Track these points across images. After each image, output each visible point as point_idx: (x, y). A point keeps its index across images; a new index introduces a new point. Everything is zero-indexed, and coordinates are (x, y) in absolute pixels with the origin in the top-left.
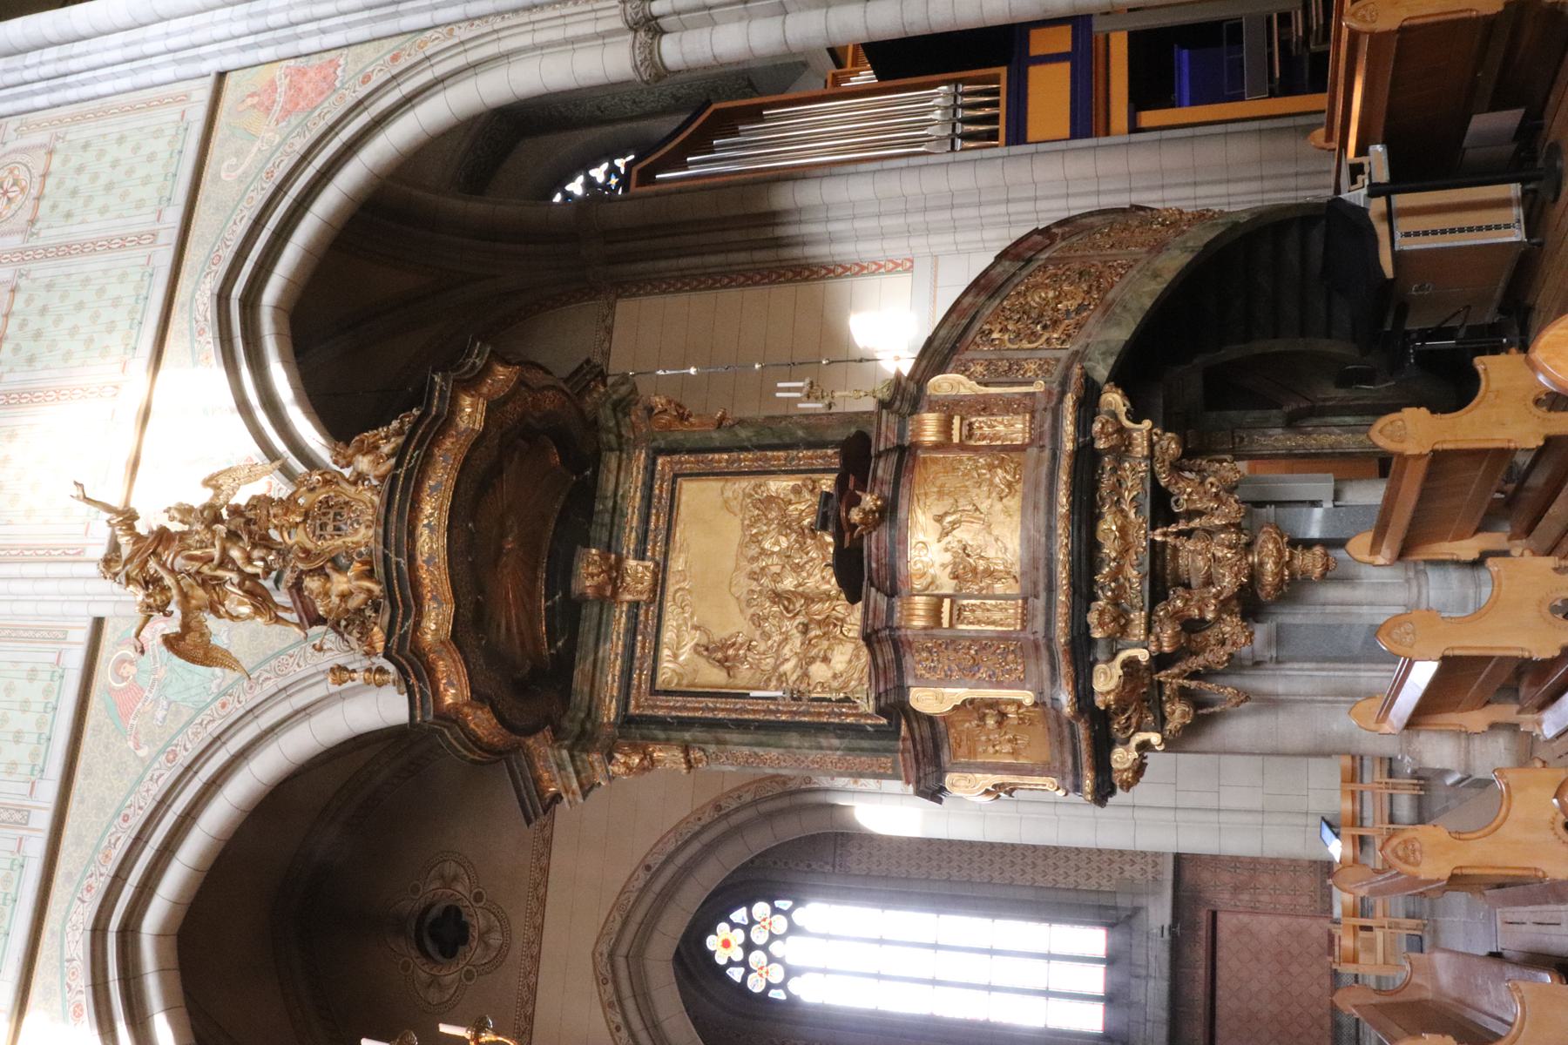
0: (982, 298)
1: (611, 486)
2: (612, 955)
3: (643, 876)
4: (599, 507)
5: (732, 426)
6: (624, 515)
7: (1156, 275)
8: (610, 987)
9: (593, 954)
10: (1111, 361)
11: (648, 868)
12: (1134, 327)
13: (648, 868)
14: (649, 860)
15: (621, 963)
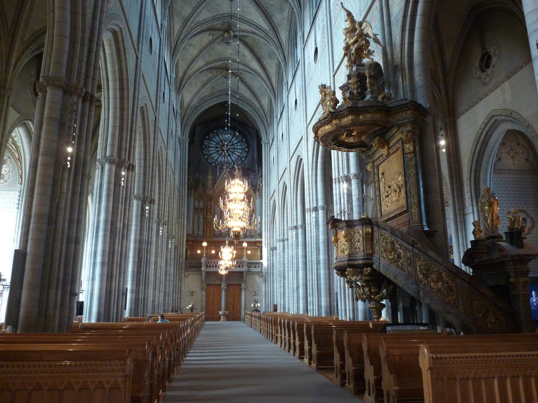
0: (390, 231)
1: (394, 132)
2: (493, 116)
3: (508, 113)
4: (390, 132)
5: (407, 157)
6: (394, 138)
7: (395, 277)
8: (487, 120)
9: (491, 111)
10: (376, 268)
11: (511, 114)
12: (383, 273)
13: (511, 114)
14: (513, 112)
15: (493, 120)
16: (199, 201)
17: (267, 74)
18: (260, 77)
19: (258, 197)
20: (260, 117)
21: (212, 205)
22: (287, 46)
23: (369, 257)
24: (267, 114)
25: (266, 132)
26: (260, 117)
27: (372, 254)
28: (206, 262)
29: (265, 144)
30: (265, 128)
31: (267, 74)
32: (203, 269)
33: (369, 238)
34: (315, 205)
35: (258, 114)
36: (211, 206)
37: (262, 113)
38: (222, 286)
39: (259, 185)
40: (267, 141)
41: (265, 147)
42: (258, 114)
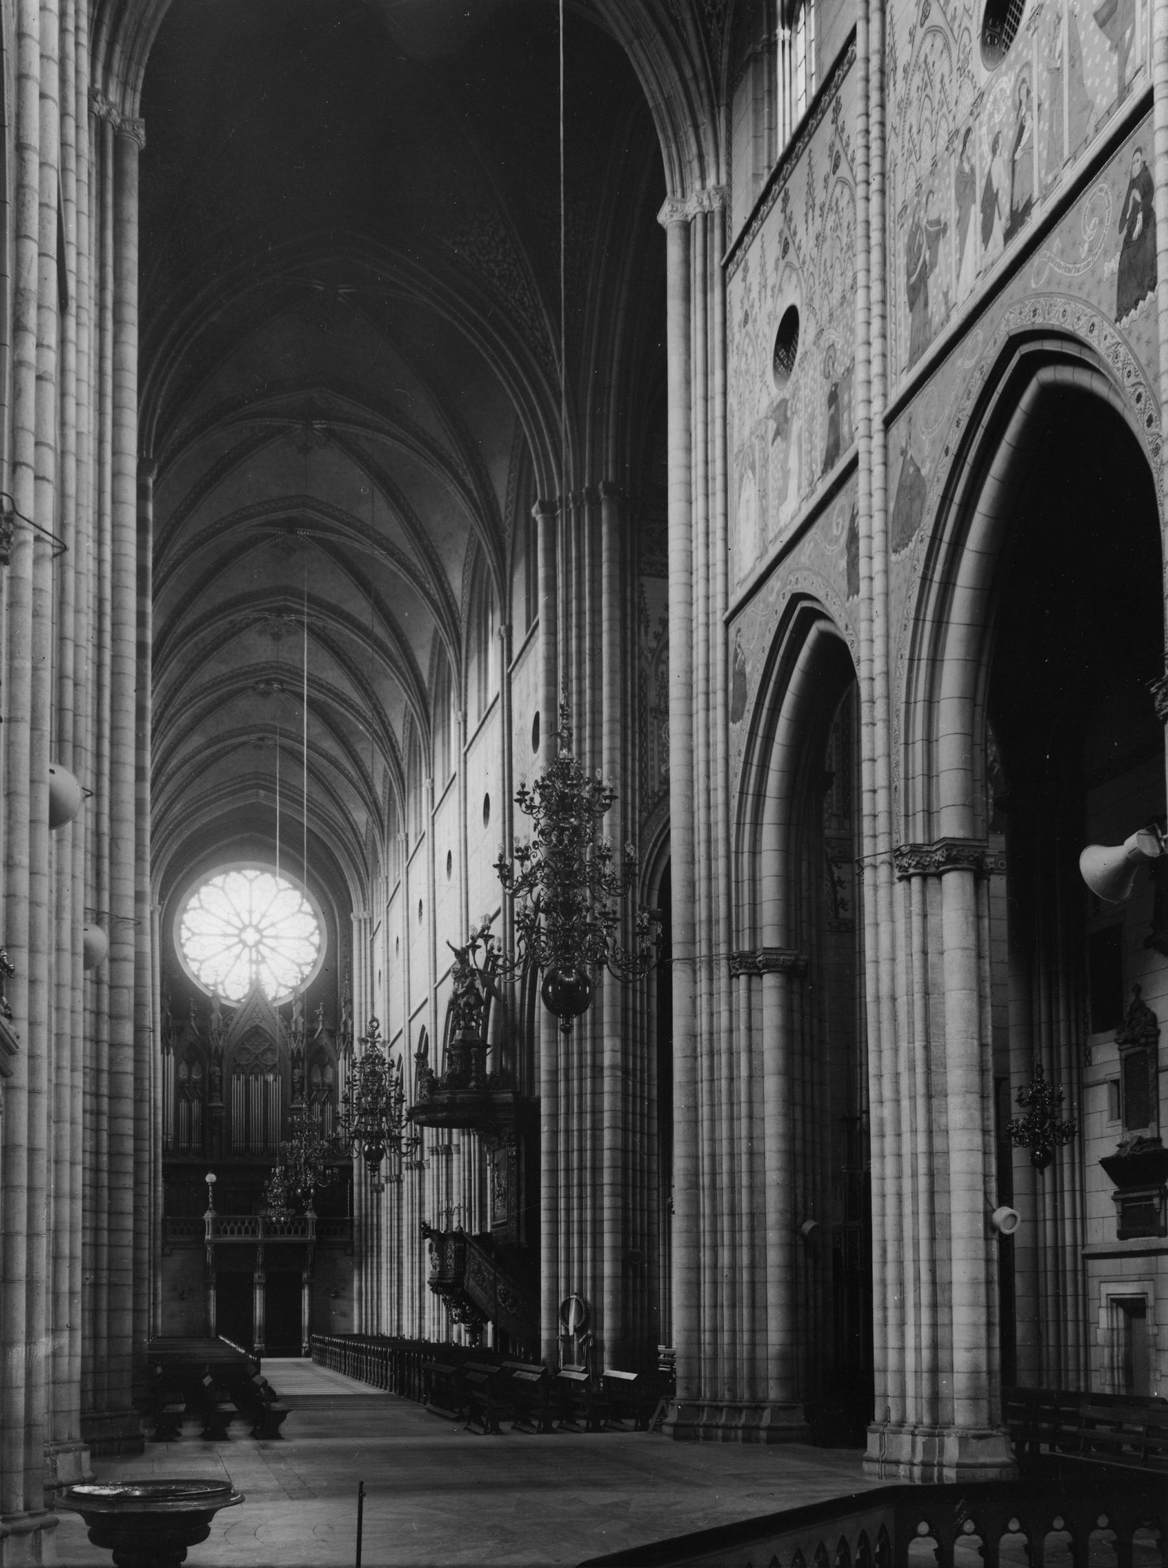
16: (190, 1064)
17: (362, 773)
18: (346, 776)
19: (342, 1055)
20: (347, 849)
21: (225, 1070)
22: (406, 752)
23: (460, 1274)
24: (366, 844)
25: (363, 890)
26: (347, 849)
27: (463, 1274)
28: (214, 1220)
29: (360, 921)
30: (360, 879)
31: (362, 773)
32: (208, 1237)
33: (461, 1256)
34: (446, 1143)
35: (341, 840)
36: (221, 1077)
37: (354, 840)
38: (256, 1275)
39: (345, 1024)
40: (366, 916)
41: (360, 931)
42: (341, 840)
